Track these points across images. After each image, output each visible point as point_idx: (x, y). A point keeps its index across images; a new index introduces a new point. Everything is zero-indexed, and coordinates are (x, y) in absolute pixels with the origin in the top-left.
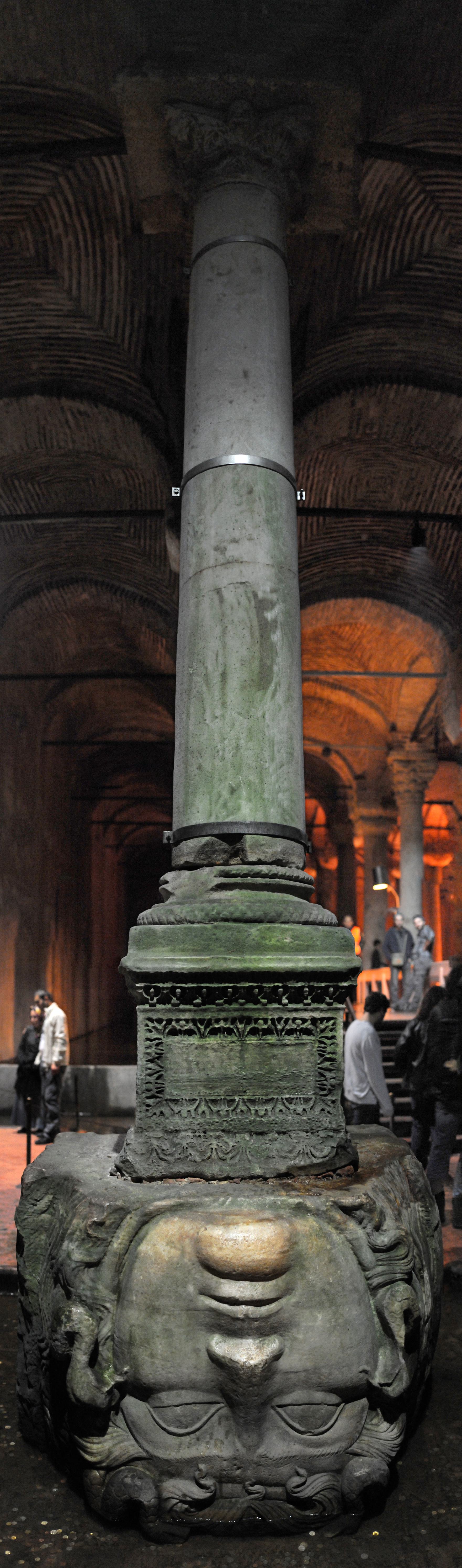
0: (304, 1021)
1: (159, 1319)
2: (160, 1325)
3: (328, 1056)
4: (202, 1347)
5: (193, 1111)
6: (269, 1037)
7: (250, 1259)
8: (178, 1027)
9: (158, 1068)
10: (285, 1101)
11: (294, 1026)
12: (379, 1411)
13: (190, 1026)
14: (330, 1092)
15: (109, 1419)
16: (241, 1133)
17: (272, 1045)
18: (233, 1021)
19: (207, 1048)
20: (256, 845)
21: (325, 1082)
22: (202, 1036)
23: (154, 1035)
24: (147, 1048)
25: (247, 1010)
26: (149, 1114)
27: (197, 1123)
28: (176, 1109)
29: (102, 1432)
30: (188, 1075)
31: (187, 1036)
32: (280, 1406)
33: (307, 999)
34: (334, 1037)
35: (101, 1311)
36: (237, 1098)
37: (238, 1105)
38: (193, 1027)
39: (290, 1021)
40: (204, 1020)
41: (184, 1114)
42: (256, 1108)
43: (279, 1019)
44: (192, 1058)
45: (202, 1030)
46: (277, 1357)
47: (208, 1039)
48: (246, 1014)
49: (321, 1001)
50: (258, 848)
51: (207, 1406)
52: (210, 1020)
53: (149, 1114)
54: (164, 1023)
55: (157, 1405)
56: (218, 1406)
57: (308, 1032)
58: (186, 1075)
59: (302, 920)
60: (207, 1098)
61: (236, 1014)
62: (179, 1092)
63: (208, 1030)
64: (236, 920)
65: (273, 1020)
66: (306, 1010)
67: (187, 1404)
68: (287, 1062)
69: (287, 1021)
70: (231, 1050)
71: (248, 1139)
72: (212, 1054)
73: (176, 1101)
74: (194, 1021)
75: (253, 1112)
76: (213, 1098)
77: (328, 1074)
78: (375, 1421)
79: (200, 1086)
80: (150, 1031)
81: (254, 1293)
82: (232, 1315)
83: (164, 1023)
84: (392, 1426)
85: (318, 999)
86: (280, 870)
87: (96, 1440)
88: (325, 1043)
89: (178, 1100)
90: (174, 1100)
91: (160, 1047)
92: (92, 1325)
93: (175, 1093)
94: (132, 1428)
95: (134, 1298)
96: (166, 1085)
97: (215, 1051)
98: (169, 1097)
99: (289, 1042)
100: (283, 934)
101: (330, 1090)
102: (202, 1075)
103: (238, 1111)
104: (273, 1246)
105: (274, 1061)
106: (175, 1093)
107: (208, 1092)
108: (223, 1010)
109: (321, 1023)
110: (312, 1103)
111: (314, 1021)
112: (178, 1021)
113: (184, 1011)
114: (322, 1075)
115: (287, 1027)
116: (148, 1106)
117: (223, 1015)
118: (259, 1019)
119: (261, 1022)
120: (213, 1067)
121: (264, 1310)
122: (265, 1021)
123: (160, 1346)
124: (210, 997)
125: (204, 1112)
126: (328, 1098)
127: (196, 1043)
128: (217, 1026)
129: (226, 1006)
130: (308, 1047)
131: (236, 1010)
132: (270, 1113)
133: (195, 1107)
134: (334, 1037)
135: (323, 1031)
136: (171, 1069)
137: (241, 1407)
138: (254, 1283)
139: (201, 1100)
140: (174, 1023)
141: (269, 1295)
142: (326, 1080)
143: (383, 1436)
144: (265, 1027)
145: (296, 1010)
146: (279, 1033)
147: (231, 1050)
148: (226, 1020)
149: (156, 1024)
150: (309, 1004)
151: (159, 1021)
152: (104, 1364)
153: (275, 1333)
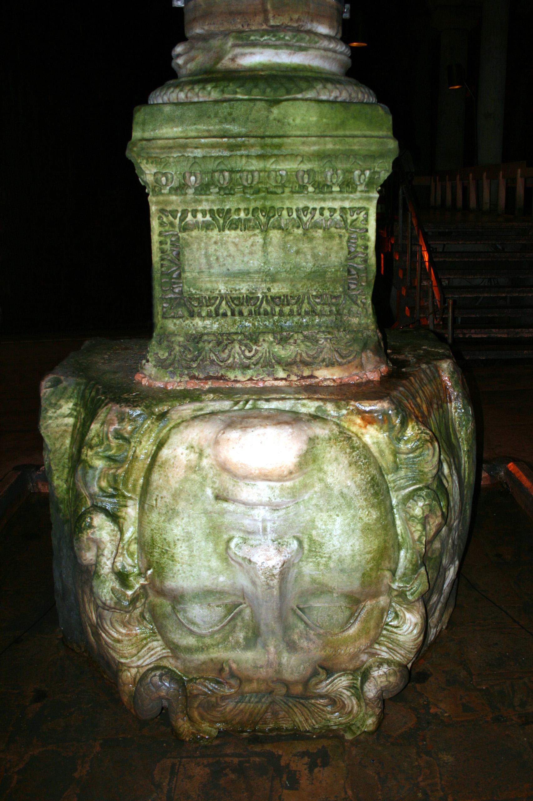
0: (333, 210)
2: (180, 528)
22: (222, 229)
37: (262, 302)
43: (306, 209)
52: (229, 211)
65: (297, 210)
66: (334, 199)
93: (194, 292)
95: (154, 502)
118: (283, 208)
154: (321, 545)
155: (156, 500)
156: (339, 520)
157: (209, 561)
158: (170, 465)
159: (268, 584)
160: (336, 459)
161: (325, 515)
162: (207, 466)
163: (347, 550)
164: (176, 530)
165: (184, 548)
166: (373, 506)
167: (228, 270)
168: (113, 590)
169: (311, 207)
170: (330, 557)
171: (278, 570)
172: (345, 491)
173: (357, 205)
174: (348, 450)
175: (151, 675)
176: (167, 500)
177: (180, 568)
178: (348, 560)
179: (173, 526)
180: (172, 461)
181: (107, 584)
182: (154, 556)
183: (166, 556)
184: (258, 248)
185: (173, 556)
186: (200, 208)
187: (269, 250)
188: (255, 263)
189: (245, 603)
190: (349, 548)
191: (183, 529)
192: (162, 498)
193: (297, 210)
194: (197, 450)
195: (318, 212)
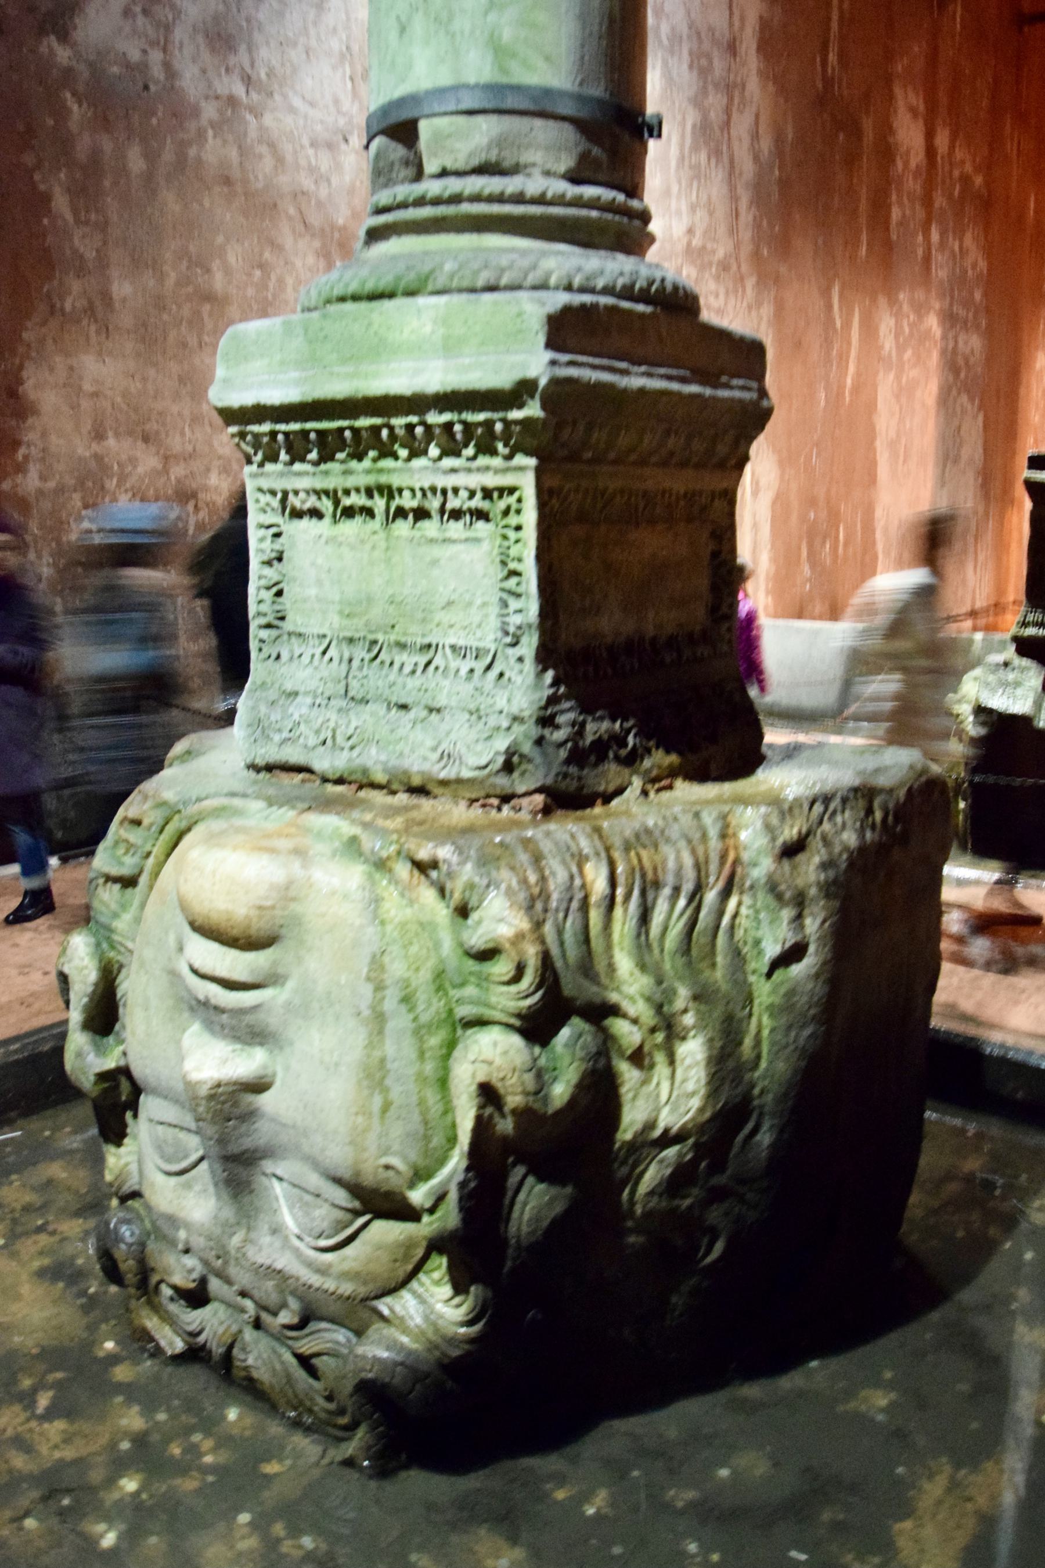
3: (513, 565)
8: (298, 504)
10: (448, 651)
13: (312, 502)
16: (375, 701)
17: (432, 541)
20: (438, 137)
25: (381, 471)
27: (319, 677)
33: (466, 446)
36: (380, 637)
39: (450, 494)
46: (259, 1086)
48: (383, 479)
49: (493, 452)
50: (451, 141)
54: (279, 495)
57: (482, 515)
58: (313, 592)
59: (480, 283)
61: (370, 480)
64: (356, 298)
65: (422, 489)
66: (469, 470)
69: (444, 492)
70: (374, 548)
74: (318, 493)
75: (396, 666)
76: (349, 634)
77: (514, 604)
78: (436, 1275)
85: (486, 448)
86: (510, 185)
90: (300, 635)
91: (281, 540)
96: (288, 606)
97: (353, 548)
100: (418, 318)
105: (436, 572)
107: (345, 622)
108: (347, 472)
109: (501, 497)
111: (487, 493)
112: (296, 493)
113: (299, 474)
115: (449, 506)
116: (262, 641)
120: (349, 577)
122: (413, 490)
124: (328, 447)
129: (354, 464)
130: (486, 546)
131: (368, 472)
134: (518, 528)
135: (506, 512)
140: (291, 496)
143: (440, 1307)
144: (414, 504)
145: (454, 471)
147: (374, 548)
149: (268, 498)
150: (474, 458)
151: (273, 493)
153: (261, 1044)
193: (422, 489)
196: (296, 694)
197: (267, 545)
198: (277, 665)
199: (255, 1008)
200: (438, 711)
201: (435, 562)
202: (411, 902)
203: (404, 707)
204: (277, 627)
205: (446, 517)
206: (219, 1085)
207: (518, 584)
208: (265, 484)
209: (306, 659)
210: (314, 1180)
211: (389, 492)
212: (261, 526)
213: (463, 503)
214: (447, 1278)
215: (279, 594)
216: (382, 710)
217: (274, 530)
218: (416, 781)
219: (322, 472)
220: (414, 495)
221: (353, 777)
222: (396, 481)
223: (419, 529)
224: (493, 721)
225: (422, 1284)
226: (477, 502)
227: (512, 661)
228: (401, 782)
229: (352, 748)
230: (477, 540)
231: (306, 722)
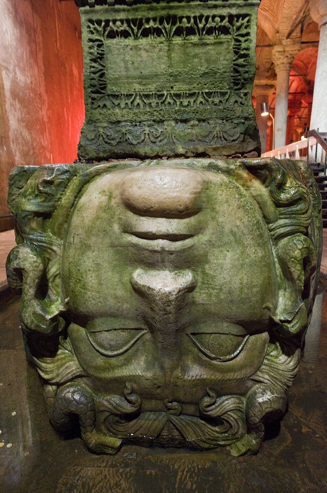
0: (222, 18)
1: (90, 255)
2: (91, 260)
3: (242, 52)
4: (126, 279)
5: (129, 104)
6: (192, 37)
7: (165, 196)
8: (115, 29)
9: (101, 68)
10: (205, 95)
11: (213, 24)
12: (278, 344)
13: (125, 27)
14: (243, 86)
15: (59, 343)
17: (194, 45)
18: (161, 23)
19: (140, 49)
21: (239, 77)
22: (136, 38)
23: (95, 37)
24: (90, 48)
26: (94, 106)
28: (116, 102)
29: (53, 353)
30: (125, 73)
31: (123, 38)
32: (193, 334)
34: (248, 34)
35: (48, 253)
37: (166, 98)
38: (127, 28)
39: (210, 19)
40: (136, 19)
41: (123, 105)
42: (181, 100)
43: (201, 17)
44: (127, 58)
45: (136, 31)
46: (190, 289)
47: (140, 40)
48: (172, 12)
51: (133, 331)
52: (141, 20)
53: (94, 106)
54: (103, 24)
55: (92, 330)
56: (143, 332)
57: (225, 30)
60: (141, 94)
61: (163, 13)
62: (119, 89)
63: (140, 31)
65: (195, 18)
66: (224, 6)
67: (115, 330)
68: (207, 61)
70: (160, 50)
71: (174, 125)
72: (144, 54)
73: (116, 96)
74: (128, 21)
75: (178, 103)
76: (146, 93)
78: (274, 353)
79: (136, 83)
80: (92, 33)
81: (169, 229)
82: (150, 248)
83: (103, 24)
84: (289, 359)
87: (49, 360)
88: (240, 41)
89: (118, 96)
90: (115, 95)
91: (101, 49)
92: (35, 262)
93: (115, 90)
94: (76, 351)
96: (108, 81)
98: (109, 93)
99: (208, 42)
101: (243, 84)
102: (137, 73)
103: (166, 103)
104: (187, 186)
105: (196, 60)
106: (115, 90)
108: (152, 9)
109: (237, 21)
110: (227, 96)
111: (231, 18)
112: (114, 21)
114: (236, 71)
116: (93, 99)
117: (151, 14)
118: (183, 17)
119: (185, 20)
121: (178, 245)
122: (188, 18)
123: (91, 280)
125: (138, 104)
126: (242, 91)
127: (131, 44)
128: (147, 26)
130: (225, 46)
132: (192, 104)
133: (131, 100)
135: (238, 29)
136: (112, 68)
137: (159, 333)
138: (169, 220)
139: (136, 95)
140: (111, 24)
141: (184, 232)
142: (240, 75)
143: (282, 367)
144: (189, 25)
146: (200, 31)
147: (160, 50)
148: (155, 20)
151: (99, 22)
152: (54, 297)
153: (189, 267)
154: (213, 277)
155: (74, 237)
156: (229, 255)
157: (115, 289)
158: (85, 208)
159: (165, 310)
160: (227, 201)
161: (216, 251)
162: (115, 205)
163: (236, 284)
164: (88, 261)
165: (93, 277)
166: (259, 245)
167: (141, 73)
168: (35, 313)
169: (206, 15)
170: (221, 289)
171: (174, 296)
172: (235, 229)
173: (243, 11)
174: (237, 196)
175: (65, 392)
176: (82, 237)
177: (91, 295)
178: (237, 292)
179: (85, 258)
180: (88, 204)
181: (29, 309)
182: (70, 286)
183: (79, 285)
184: (163, 53)
185: (84, 285)
186: (119, 18)
187: (172, 56)
188: (162, 67)
189: (146, 329)
190: (238, 281)
191: (93, 261)
192: (78, 235)
193: (195, 18)
194: (108, 193)
195: (210, 19)
196: (119, 122)
197: (95, 50)
198: (105, 110)
199: (191, 248)
200: (204, 121)
201: (195, 56)
202: (248, 188)
203: (185, 121)
204: (101, 93)
205: (204, 33)
206: (179, 291)
207: (244, 61)
208: (95, 17)
209: (123, 105)
210: (225, 327)
211: (173, 19)
212: (91, 40)
213: (217, 24)
214: (281, 352)
215: (102, 75)
216: (173, 123)
217: (97, 43)
218: (201, 149)
219: (133, 9)
220: (189, 22)
221: (165, 153)
222: (179, 13)
223: (188, 40)
224: (236, 121)
225: (268, 360)
226: (225, 22)
227: (242, 95)
228: (193, 153)
229: (160, 141)
230: (221, 43)
231: (130, 133)
